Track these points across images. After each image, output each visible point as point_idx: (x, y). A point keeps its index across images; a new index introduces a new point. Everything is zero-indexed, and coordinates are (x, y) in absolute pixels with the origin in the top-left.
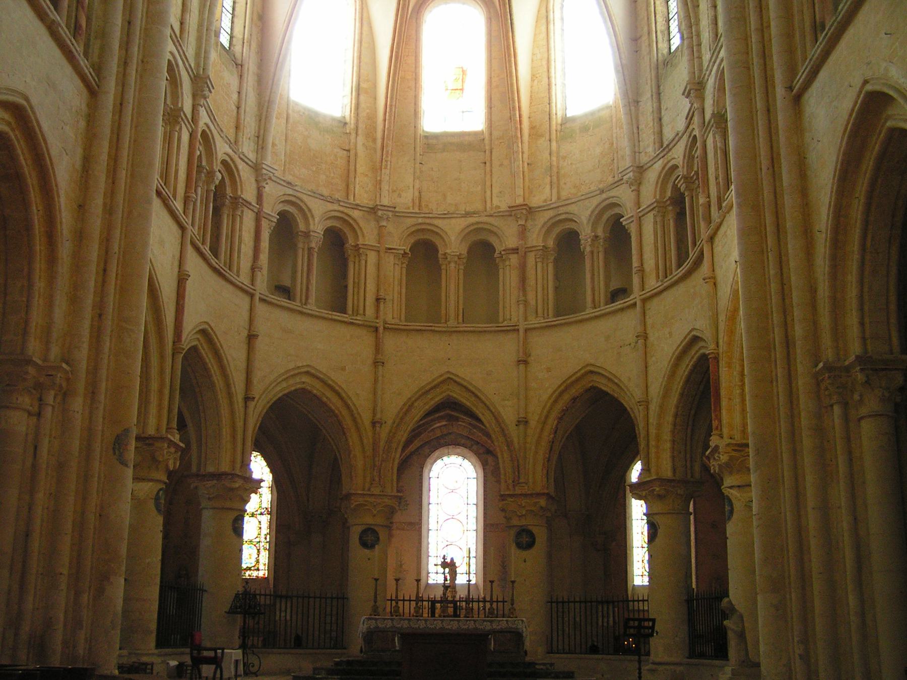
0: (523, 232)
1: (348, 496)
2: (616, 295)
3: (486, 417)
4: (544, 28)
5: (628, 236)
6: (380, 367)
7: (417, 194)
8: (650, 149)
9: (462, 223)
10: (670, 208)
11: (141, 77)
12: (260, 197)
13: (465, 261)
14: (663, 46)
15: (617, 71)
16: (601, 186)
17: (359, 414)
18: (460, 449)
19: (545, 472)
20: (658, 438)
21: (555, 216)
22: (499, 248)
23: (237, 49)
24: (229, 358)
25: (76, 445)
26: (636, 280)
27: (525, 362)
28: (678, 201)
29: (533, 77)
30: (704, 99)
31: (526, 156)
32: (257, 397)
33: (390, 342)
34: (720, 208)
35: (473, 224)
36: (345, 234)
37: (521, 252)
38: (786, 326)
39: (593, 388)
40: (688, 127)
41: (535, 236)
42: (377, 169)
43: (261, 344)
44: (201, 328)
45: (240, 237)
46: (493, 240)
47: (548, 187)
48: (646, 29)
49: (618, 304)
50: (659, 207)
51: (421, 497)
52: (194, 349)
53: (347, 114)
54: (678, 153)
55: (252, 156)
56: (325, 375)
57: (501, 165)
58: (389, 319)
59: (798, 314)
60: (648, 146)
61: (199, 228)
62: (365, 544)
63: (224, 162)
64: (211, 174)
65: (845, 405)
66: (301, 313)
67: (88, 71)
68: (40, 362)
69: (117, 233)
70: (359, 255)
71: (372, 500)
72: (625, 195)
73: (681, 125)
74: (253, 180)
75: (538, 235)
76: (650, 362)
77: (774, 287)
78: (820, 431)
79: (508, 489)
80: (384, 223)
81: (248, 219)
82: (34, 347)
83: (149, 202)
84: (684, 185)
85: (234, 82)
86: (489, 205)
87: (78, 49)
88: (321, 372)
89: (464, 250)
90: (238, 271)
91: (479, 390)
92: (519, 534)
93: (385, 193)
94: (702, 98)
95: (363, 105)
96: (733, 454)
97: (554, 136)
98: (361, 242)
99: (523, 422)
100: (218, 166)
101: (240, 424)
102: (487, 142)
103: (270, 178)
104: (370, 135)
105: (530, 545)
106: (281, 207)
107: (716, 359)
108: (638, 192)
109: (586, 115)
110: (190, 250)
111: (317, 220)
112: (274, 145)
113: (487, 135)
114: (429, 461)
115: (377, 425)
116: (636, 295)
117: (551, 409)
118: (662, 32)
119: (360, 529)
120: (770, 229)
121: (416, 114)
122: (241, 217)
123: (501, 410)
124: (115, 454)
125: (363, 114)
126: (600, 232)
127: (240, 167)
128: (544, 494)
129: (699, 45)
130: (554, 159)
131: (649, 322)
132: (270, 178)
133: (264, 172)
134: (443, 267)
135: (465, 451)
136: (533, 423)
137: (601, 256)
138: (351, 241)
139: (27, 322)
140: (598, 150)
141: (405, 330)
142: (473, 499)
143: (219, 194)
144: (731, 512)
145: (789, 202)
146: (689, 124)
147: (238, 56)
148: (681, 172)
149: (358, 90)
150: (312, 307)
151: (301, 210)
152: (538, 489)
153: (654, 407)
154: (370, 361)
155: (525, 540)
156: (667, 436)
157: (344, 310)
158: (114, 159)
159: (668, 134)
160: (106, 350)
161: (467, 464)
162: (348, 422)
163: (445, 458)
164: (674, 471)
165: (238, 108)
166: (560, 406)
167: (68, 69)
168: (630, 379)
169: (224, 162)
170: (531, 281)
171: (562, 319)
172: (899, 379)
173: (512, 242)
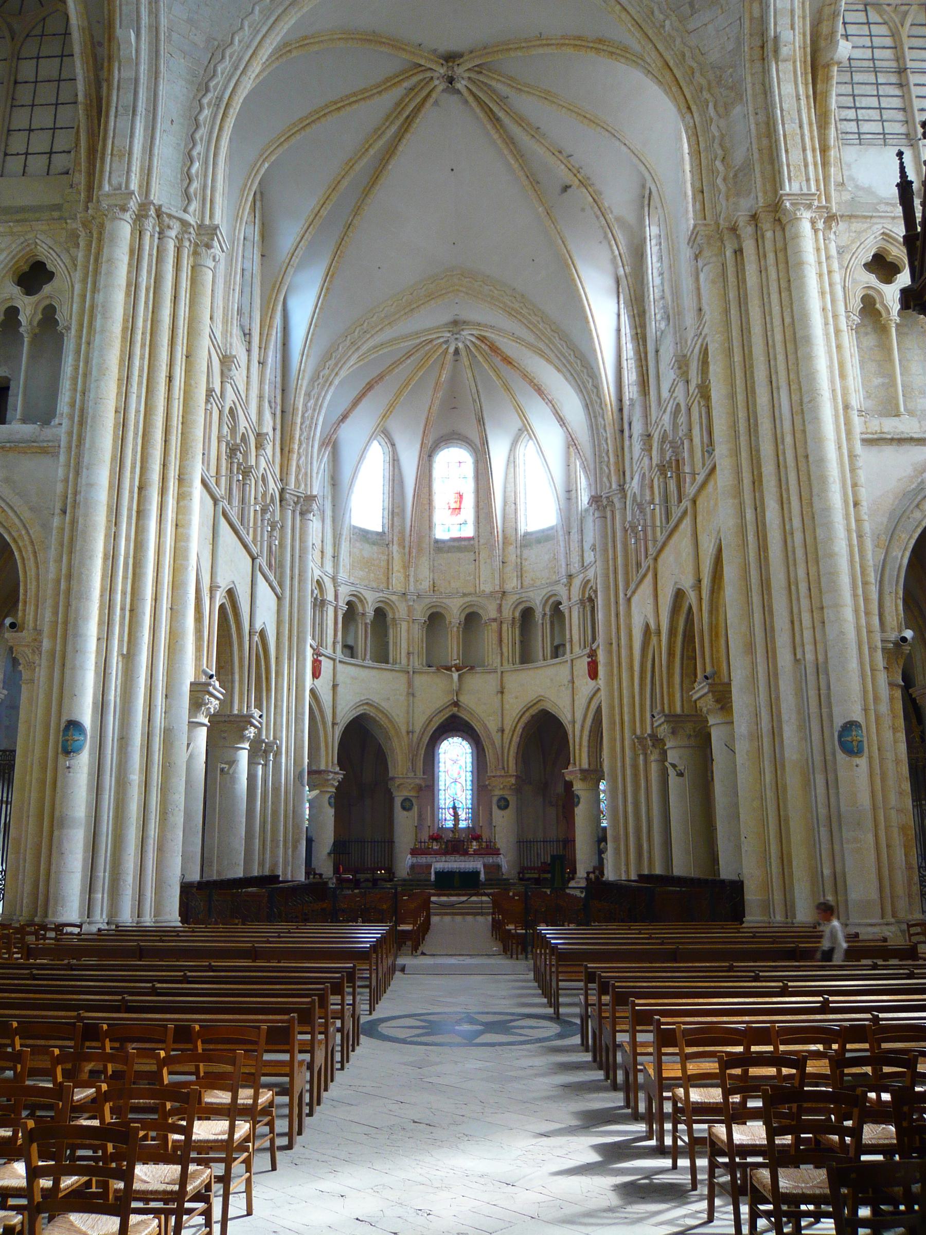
0: (500, 609)
1: (393, 779)
2: (557, 651)
3: (477, 727)
4: (512, 470)
5: (564, 616)
8: (576, 565)
22: (485, 618)
27: (502, 693)
29: (505, 503)
33: (419, 681)
43: (340, 689)
46: (481, 612)
50: (582, 602)
51: (433, 768)
53: (386, 530)
62: (404, 808)
65: (645, 755)
71: (408, 780)
72: (562, 592)
73: (593, 559)
76: (576, 698)
77: (616, 694)
78: (635, 766)
80: (411, 603)
81: (330, 611)
87: (272, 578)
89: (463, 619)
92: (499, 801)
93: (412, 584)
95: (396, 523)
101: (330, 740)
104: (402, 544)
105: (506, 807)
106: (348, 599)
108: (569, 590)
116: (568, 656)
117: (519, 720)
119: (402, 798)
120: (615, 664)
123: (486, 722)
126: (547, 609)
130: (519, 560)
131: (575, 673)
135: (464, 735)
136: (507, 732)
137: (548, 626)
138: (390, 616)
140: (547, 557)
142: (469, 768)
149: (393, 514)
150: (369, 663)
151: (361, 601)
153: (578, 726)
154: (405, 693)
156: (585, 743)
157: (387, 662)
161: (465, 743)
162: (392, 733)
164: (589, 764)
170: (505, 641)
173: (493, 614)
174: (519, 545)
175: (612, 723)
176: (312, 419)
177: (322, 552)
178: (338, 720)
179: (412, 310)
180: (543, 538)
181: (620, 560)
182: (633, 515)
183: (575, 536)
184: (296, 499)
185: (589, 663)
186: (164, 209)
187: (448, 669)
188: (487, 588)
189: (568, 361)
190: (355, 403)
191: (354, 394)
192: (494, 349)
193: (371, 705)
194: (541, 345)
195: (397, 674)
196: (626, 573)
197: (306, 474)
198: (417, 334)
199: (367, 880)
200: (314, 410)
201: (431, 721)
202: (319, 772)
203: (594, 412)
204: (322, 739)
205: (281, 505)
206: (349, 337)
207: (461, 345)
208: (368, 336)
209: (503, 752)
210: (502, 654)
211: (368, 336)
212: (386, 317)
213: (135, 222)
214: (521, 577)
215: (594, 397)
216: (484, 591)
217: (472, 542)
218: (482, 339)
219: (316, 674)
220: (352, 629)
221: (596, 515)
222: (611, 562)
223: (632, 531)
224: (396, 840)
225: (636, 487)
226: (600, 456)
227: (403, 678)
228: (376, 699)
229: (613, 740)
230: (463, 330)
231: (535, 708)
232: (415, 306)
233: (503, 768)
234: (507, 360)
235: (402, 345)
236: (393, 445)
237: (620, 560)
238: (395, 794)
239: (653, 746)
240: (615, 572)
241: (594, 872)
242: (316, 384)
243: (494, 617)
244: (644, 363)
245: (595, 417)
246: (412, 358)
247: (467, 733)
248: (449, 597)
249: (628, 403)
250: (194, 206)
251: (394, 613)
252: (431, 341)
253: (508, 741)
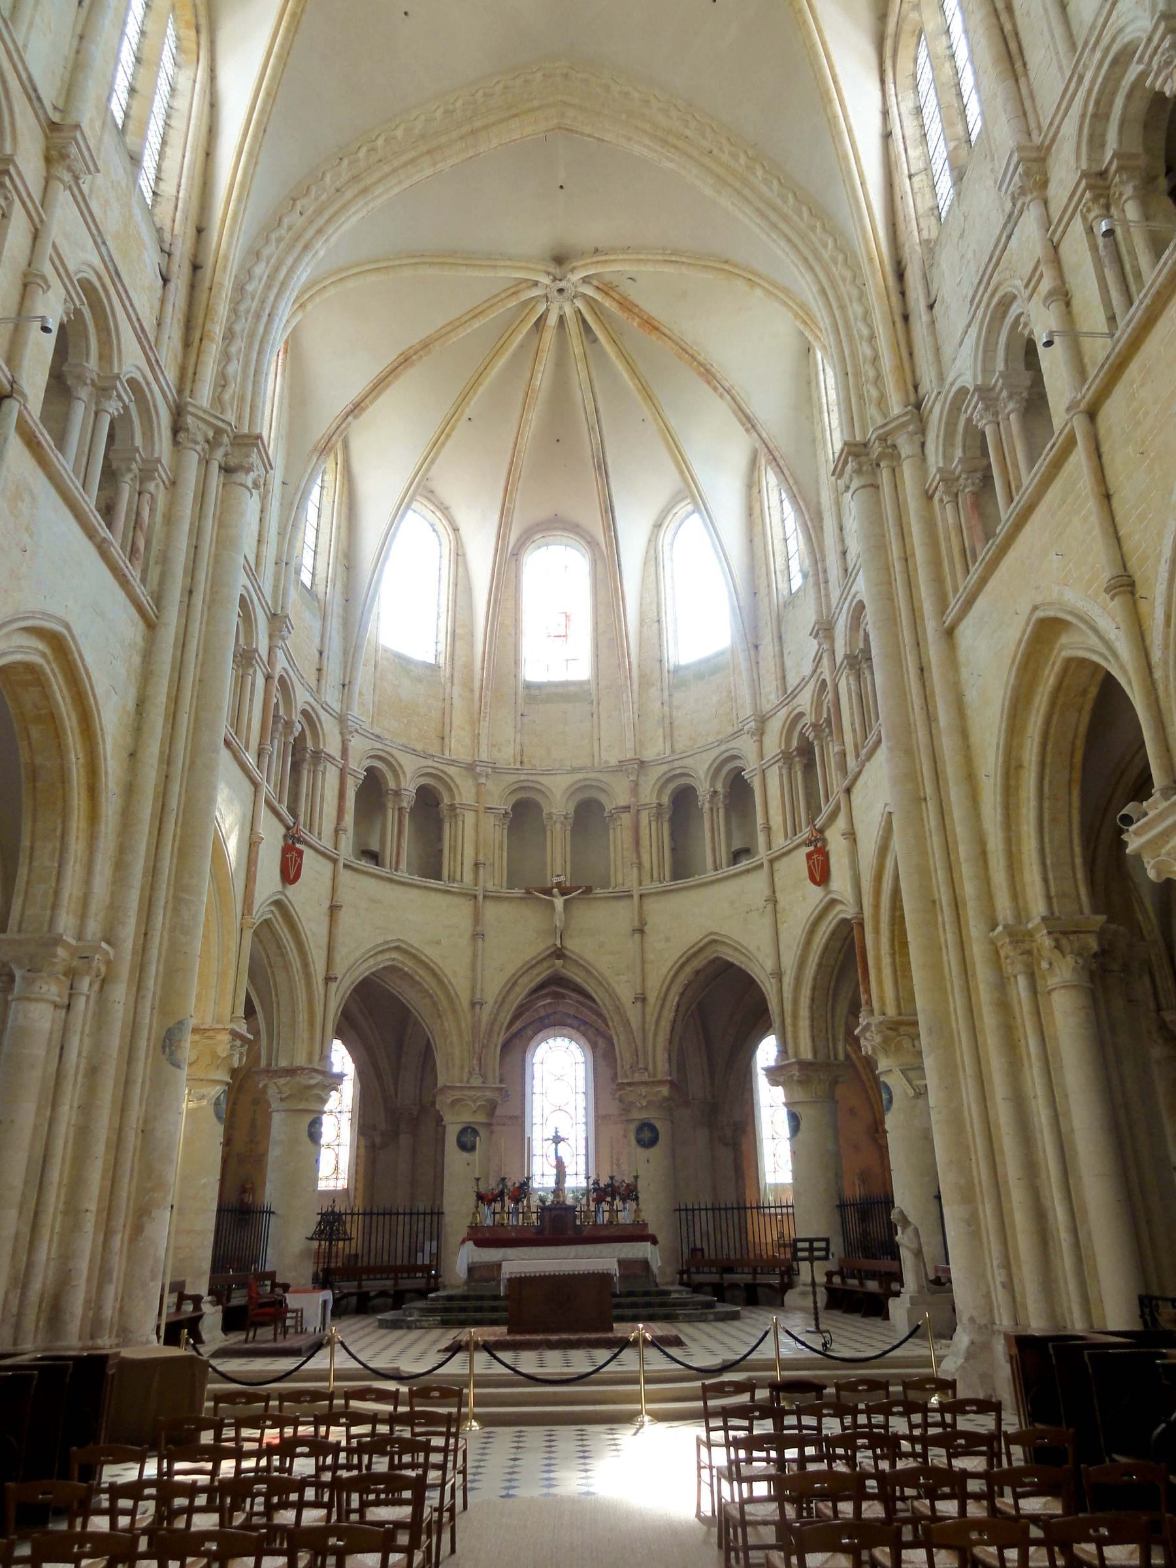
0: (635, 788)
2: (736, 856)
3: (598, 994)
4: (652, 570)
6: (480, 941)
7: (518, 748)
8: (773, 696)
9: (568, 780)
10: (797, 759)
11: (209, 608)
12: (344, 752)
13: (571, 821)
14: (783, 586)
15: (734, 614)
16: (720, 737)
17: (456, 994)
18: (567, 1030)
19: (666, 1055)
20: (795, 1016)
21: (670, 771)
22: (609, 806)
23: (320, 589)
24: (309, 934)
25: (115, 1042)
26: (761, 839)
27: (642, 931)
28: (806, 751)
29: (642, 622)
30: (833, 641)
31: (636, 706)
32: (340, 977)
33: (491, 911)
34: (857, 756)
35: (580, 781)
36: (440, 793)
37: (633, 811)
38: (952, 884)
39: (718, 958)
40: (815, 671)
41: (648, 792)
42: (475, 721)
43: (344, 916)
44: (275, 898)
45: (322, 796)
46: (602, 798)
47: (661, 739)
48: (764, 569)
49: (744, 864)
50: (786, 757)
52: (267, 922)
53: (442, 661)
54: (805, 701)
55: (336, 706)
56: (417, 949)
57: (609, 717)
58: (490, 886)
59: (966, 869)
60: (770, 693)
61: (275, 785)
63: (304, 713)
64: (289, 724)
65: (1032, 977)
66: (391, 881)
67: (145, 600)
68: (73, 942)
69: (176, 788)
70: (456, 816)
71: (472, 1093)
72: (747, 746)
73: (807, 669)
74: (337, 732)
75: (652, 791)
76: (782, 928)
77: (936, 841)
78: (1004, 1006)
79: (627, 1077)
80: (483, 780)
82: (66, 923)
83: (216, 750)
84: (813, 734)
85: (317, 625)
86: (596, 758)
87: (134, 574)
88: (412, 947)
89: (571, 809)
90: (319, 834)
91: (589, 963)
92: (640, 1130)
93: (484, 748)
94: (831, 639)
95: (458, 652)
96: (890, 1033)
97: (665, 686)
98: (457, 801)
99: (642, 999)
100: (297, 717)
102: (594, 692)
103: (357, 731)
105: (652, 1142)
106: (368, 763)
107: (861, 925)
108: (761, 742)
109: (700, 662)
110: (263, 809)
111: (409, 776)
112: (360, 694)
113: (593, 684)
114: (533, 1044)
115: (478, 1007)
116: (762, 854)
117: (672, 982)
118: (781, 572)
119: (457, 1128)
121: (517, 662)
122: (324, 773)
123: (614, 985)
124: (164, 1052)
125: (459, 663)
126: (719, 787)
127: (323, 719)
128: (665, 1082)
129: (826, 582)
130: (666, 709)
132: (357, 731)
133: (350, 723)
134: (548, 828)
135: (573, 1032)
136: (652, 998)
138: (446, 801)
139: (57, 893)
141: (507, 898)
142: (581, 1087)
143: (298, 747)
144: (890, 1101)
145: (948, 744)
146: (817, 667)
147: (321, 595)
148: (809, 719)
150: (403, 875)
152: (660, 1077)
153: (788, 980)
155: (647, 1136)
156: (804, 1013)
157: (438, 876)
158: (175, 700)
159: (792, 681)
160: (159, 926)
161: (574, 1046)
162: (444, 1003)
163: (551, 1041)
164: (815, 1052)
165: (321, 653)
166: (682, 979)
167: (121, 595)
168: (758, 948)
169: (304, 713)
170: (645, 841)
171: (681, 883)
172: (1094, 945)
173: (623, 799)
174: (665, 686)
175: (931, 904)
176: (263, 302)
177: (319, 670)
178: (339, 970)
180: (708, 670)
181: (920, 555)
182: (947, 457)
183: (768, 650)
184: (211, 434)
185: (809, 856)
187: (548, 892)
188: (612, 758)
190: (379, 385)
191: (375, 369)
192: (626, 305)
193: (405, 952)
195: (457, 900)
196: (938, 579)
197: (242, 399)
199: (383, 1294)
200: (268, 287)
201: (516, 981)
202: (291, 1072)
203: (839, 298)
204: (302, 1005)
205: (176, 442)
206: (346, 162)
207: (568, 311)
208: (386, 169)
209: (644, 1039)
210: (640, 866)
211: (386, 169)
212: (423, 137)
214: (670, 736)
215: (838, 271)
216: (607, 762)
217: (586, 687)
219: (290, 872)
220: (378, 825)
221: (855, 484)
222: (898, 567)
223: (947, 492)
224: (446, 1209)
225: (970, 362)
226: (857, 374)
227: (466, 906)
228: (414, 940)
229: (934, 947)
230: (572, 270)
231: (701, 956)
232: (478, 124)
233: (646, 1069)
234: (651, 325)
236: (456, 530)
237: (920, 555)
238: (448, 1118)
239: (1058, 947)
240: (910, 584)
241: (840, 1273)
242: (274, 236)
243: (625, 803)
244: (1004, 17)
245: (842, 308)
247: (578, 1029)
248: (548, 773)
249: (918, 248)
251: (452, 796)
253: (654, 1019)
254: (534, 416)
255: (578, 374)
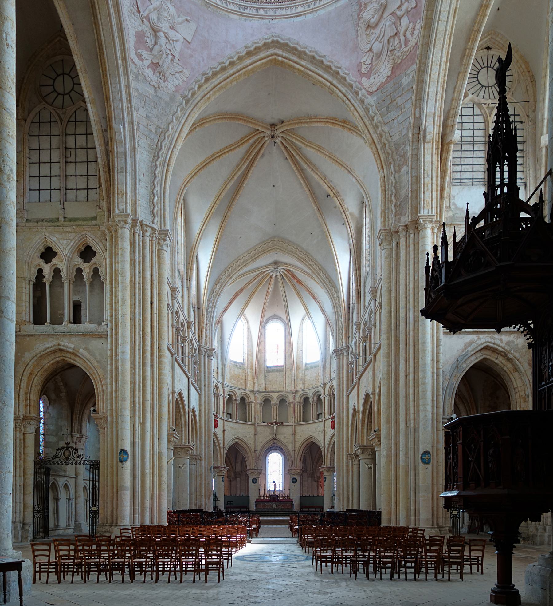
0: (294, 397)
22: (288, 401)
46: (286, 399)
92: (293, 479)
105: (296, 482)
136: (296, 450)
155: (294, 481)
170: (296, 412)
173: (291, 400)
179: (255, 258)
186: (143, 222)
189: (326, 284)
192: (293, 276)
194: (314, 276)
198: (258, 269)
207: (278, 274)
210: (295, 418)
212: (244, 262)
213: (131, 228)
218: (288, 271)
234: (299, 282)
235: (251, 274)
246: (256, 281)
250: (157, 219)
252: (264, 272)
254: (269, 298)
255: (281, 288)
